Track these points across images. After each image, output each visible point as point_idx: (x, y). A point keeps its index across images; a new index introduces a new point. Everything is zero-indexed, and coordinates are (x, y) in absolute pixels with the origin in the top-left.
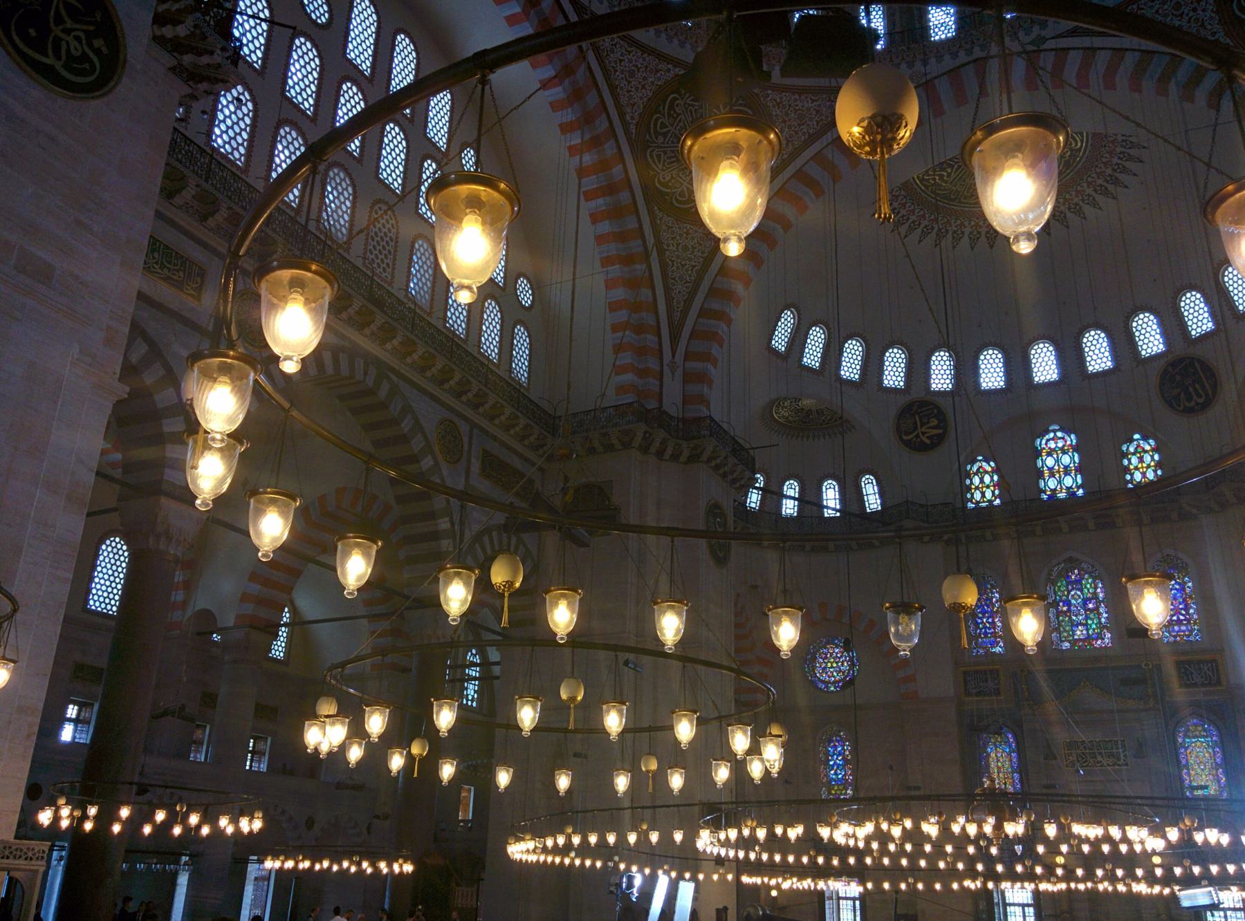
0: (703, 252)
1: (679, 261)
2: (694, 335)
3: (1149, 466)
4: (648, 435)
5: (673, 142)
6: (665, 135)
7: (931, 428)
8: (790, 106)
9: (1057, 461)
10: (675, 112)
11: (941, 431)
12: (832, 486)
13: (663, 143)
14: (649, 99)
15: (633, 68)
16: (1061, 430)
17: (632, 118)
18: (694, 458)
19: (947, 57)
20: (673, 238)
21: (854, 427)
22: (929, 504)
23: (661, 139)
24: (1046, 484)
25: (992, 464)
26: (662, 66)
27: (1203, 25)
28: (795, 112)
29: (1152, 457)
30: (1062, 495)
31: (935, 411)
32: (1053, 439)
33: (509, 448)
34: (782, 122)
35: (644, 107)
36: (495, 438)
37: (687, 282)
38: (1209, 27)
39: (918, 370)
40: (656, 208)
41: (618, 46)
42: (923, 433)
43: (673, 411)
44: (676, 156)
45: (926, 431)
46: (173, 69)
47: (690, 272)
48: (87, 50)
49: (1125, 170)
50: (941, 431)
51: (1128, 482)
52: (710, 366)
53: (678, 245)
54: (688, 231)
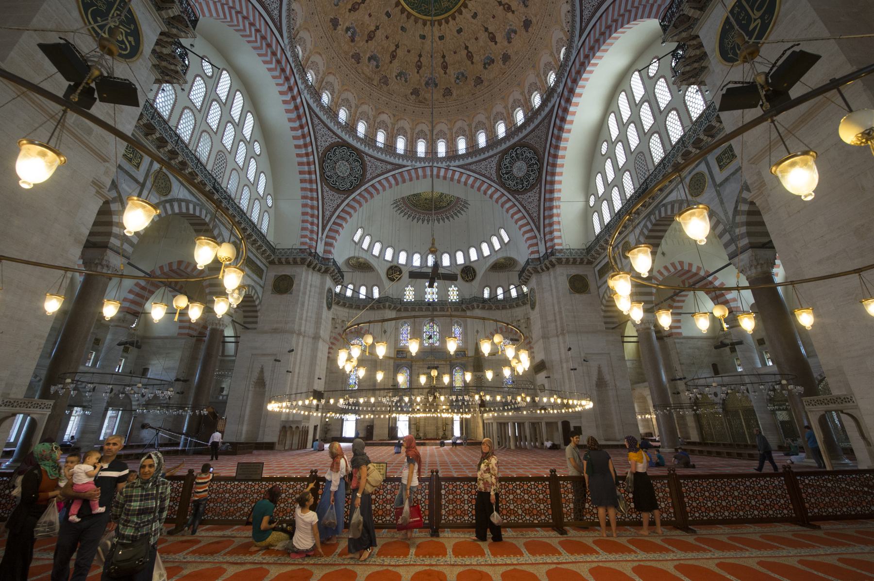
2: (330, 230)
6: (331, 160)
18: (326, 271)
23: (329, 161)
26: (334, 136)
33: (256, 257)
36: (252, 252)
39: (396, 255)
43: (321, 255)
46: (154, 66)
48: (125, 39)
49: (463, 210)
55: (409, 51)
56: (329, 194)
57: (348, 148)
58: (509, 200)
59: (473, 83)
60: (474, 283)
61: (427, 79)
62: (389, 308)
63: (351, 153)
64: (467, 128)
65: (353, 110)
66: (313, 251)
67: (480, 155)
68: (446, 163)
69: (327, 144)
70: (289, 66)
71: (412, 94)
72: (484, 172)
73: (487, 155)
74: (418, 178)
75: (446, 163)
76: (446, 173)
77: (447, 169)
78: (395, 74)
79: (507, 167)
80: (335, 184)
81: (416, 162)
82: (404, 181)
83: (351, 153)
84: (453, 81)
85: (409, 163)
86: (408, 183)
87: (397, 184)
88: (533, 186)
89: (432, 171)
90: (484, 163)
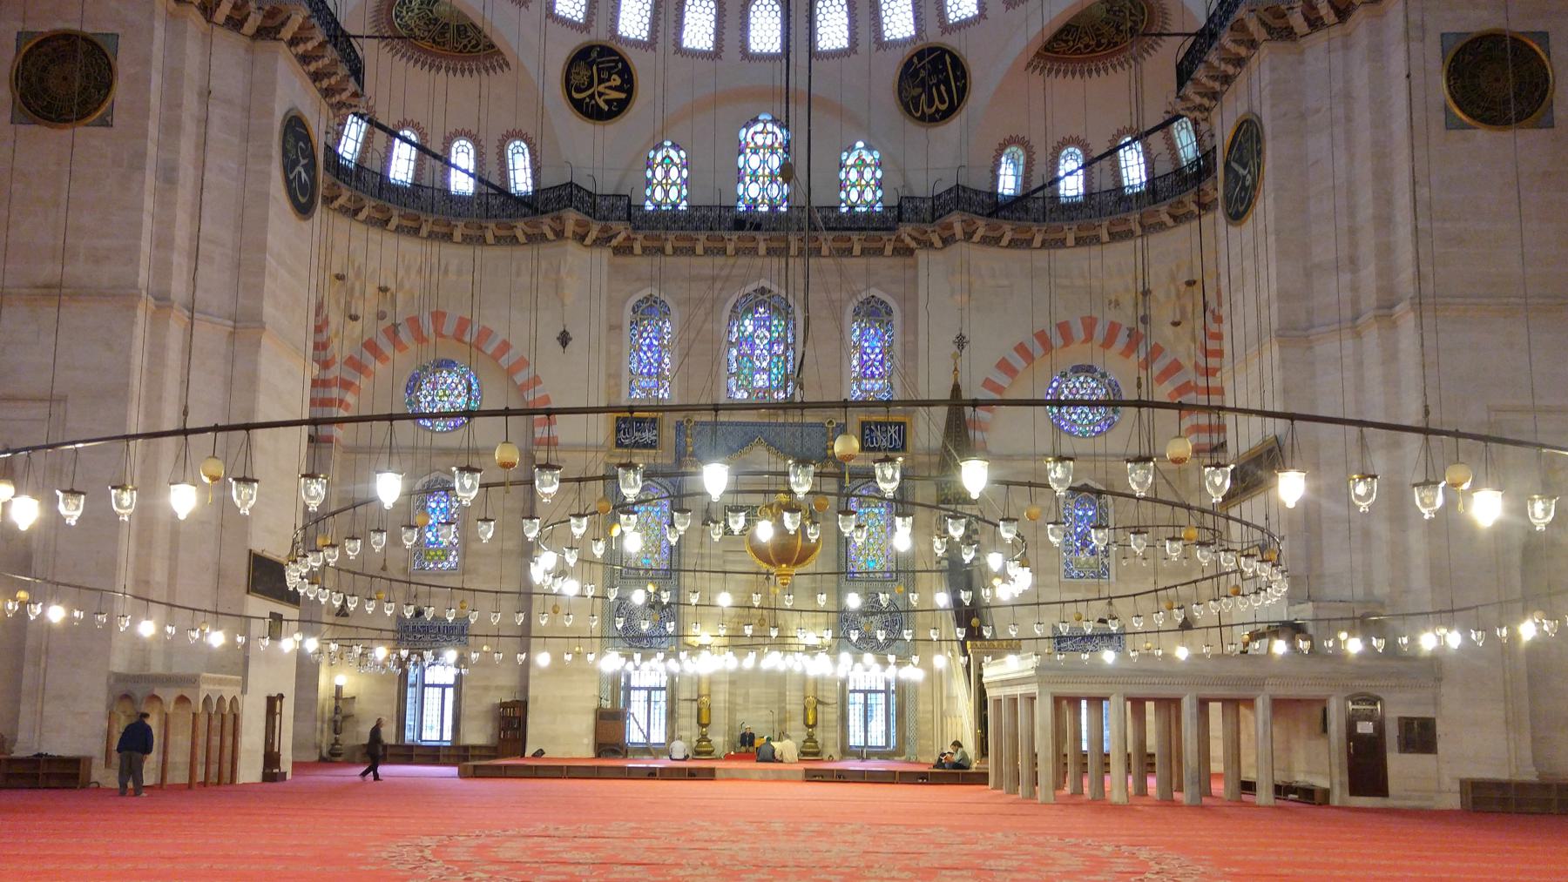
3: (868, 184)
7: (610, 88)
9: (764, 162)
11: (623, 96)
12: (466, 150)
16: (774, 121)
21: (508, 65)
22: (598, 192)
24: (746, 189)
25: (683, 154)
29: (874, 173)
30: (764, 209)
31: (620, 65)
32: (762, 132)
42: (600, 94)
45: (608, 91)
50: (623, 96)
51: (842, 201)
60: (955, 124)
62: (581, 238)
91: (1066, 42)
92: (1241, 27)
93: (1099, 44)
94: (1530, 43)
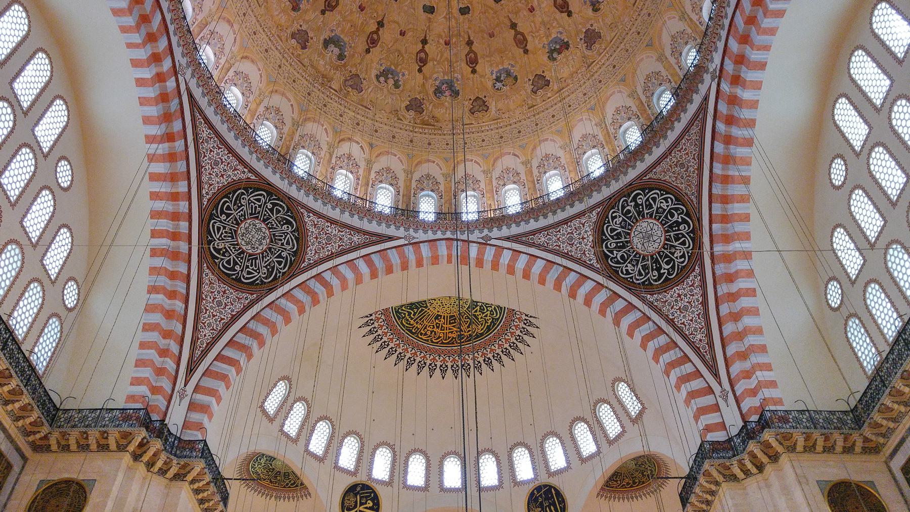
0: (233, 311)
1: (212, 311)
4: (145, 440)
5: (232, 223)
6: (228, 215)
8: (323, 229)
10: (240, 203)
13: (225, 220)
14: (224, 186)
15: (219, 160)
17: (207, 193)
19: (430, 232)
20: (212, 292)
23: (224, 217)
26: (240, 167)
27: (584, 253)
28: (326, 234)
34: (315, 238)
35: (218, 190)
37: (213, 329)
38: (588, 256)
40: (205, 265)
41: (212, 140)
44: (232, 233)
47: (218, 322)
52: (213, 400)
53: (215, 298)
54: (225, 291)
55: (403, 34)
56: (215, 287)
57: (269, 194)
58: (631, 307)
59: (529, 87)
61: (437, 83)
63: (274, 205)
64: (522, 169)
65: (286, 130)
66: (155, 417)
67: (554, 213)
68: (481, 231)
69: (224, 181)
70: (159, 17)
71: (408, 108)
72: (565, 248)
73: (570, 211)
74: (419, 264)
75: (481, 231)
76: (481, 254)
77: (484, 243)
78: (374, 72)
79: (619, 235)
80: (233, 269)
81: (416, 231)
82: (389, 270)
83: (274, 205)
84: (489, 84)
85: (401, 232)
86: (398, 273)
87: (374, 275)
88: (683, 273)
89: (449, 248)
90: (564, 229)
91: (617, 481)
92: (707, 474)
93: (634, 483)
94: (863, 486)
